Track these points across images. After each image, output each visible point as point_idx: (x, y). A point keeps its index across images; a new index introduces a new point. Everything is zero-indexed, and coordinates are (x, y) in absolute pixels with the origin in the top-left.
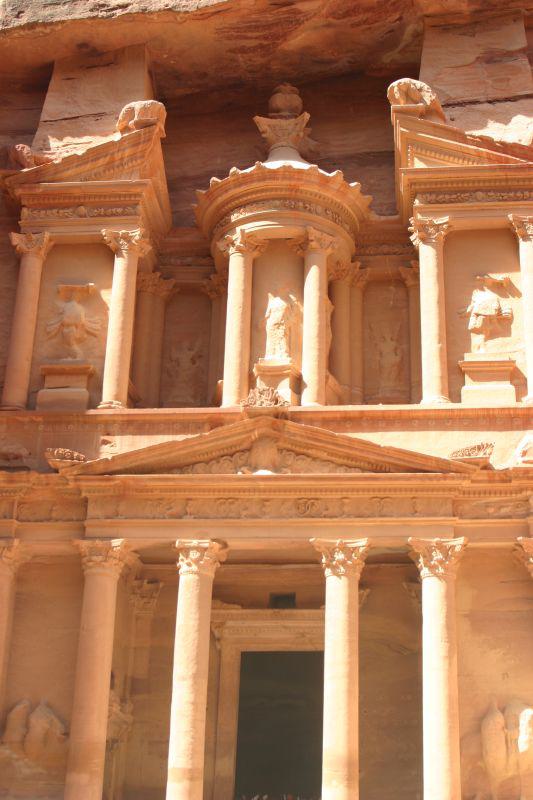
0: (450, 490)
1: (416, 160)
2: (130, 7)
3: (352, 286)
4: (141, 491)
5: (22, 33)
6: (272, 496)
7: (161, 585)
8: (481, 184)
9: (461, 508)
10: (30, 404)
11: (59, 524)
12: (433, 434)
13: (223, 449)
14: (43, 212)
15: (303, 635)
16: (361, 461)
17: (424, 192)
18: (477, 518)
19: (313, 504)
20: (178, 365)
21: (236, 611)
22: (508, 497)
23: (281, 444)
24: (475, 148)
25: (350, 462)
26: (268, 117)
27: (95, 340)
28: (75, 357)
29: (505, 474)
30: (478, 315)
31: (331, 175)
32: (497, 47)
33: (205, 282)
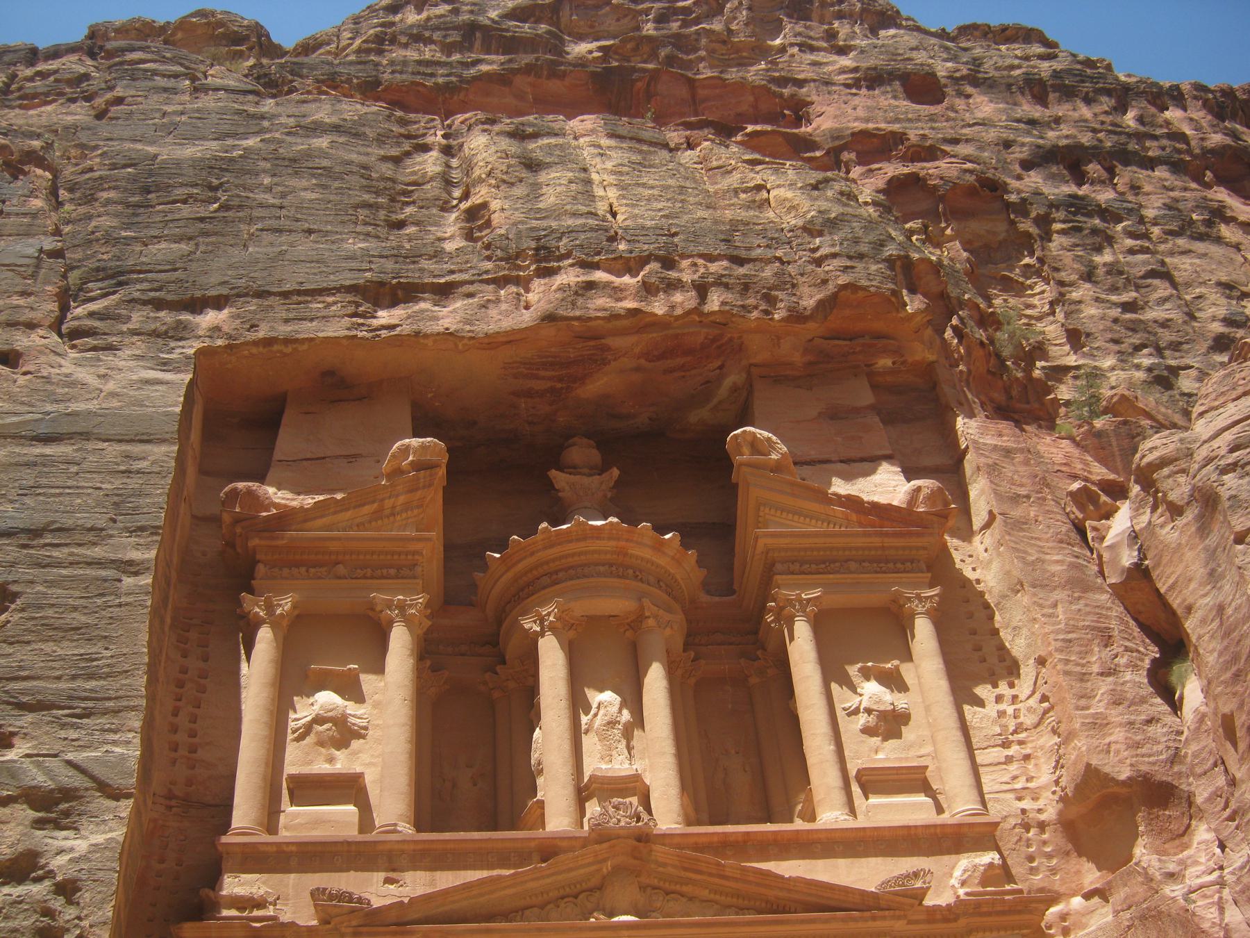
5: (254, 350)
8: (854, 552)
14: (286, 571)
27: (362, 741)
30: (869, 711)
31: (667, 537)
33: (488, 675)
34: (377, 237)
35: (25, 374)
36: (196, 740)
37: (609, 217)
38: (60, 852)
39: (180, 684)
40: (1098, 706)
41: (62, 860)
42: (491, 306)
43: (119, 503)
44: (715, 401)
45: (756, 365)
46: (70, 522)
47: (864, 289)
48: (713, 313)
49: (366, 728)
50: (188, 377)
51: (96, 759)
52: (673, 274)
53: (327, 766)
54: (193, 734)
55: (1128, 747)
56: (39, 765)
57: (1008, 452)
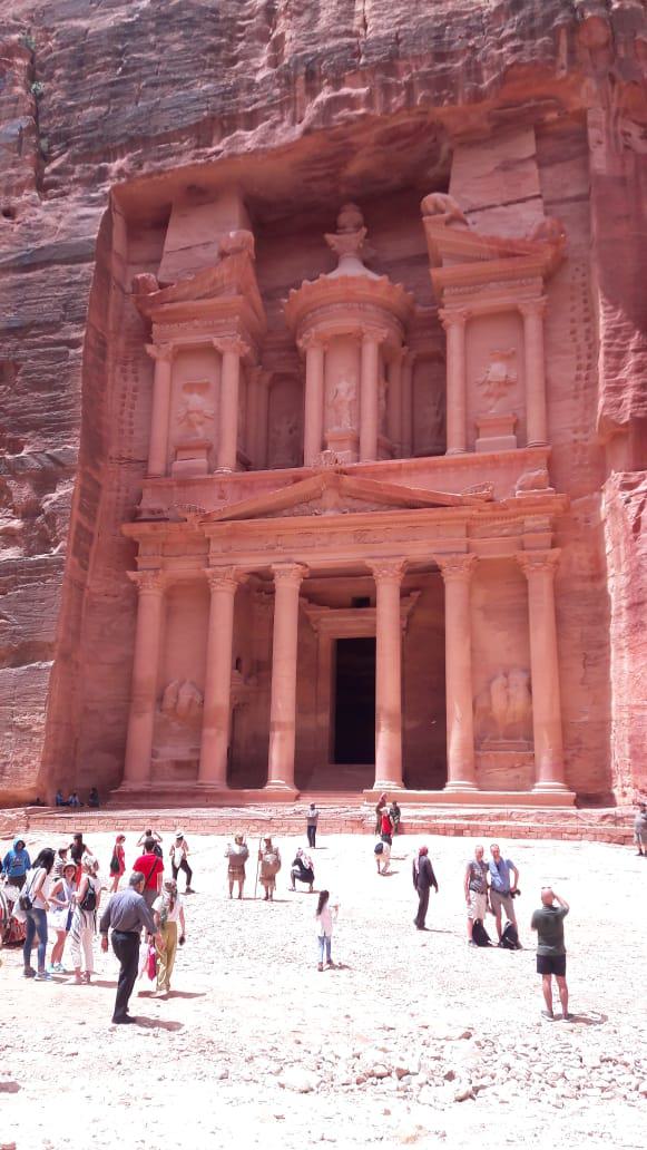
3: (403, 365)
10: (167, 474)
11: (193, 557)
21: (326, 610)
22: (508, 521)
30: (490, 382)
33: (296, 371)
34: (216, 77)
35: (18, 223)
37: (362, 31)
38: (47, 500)
40: (623, 375)
41: (47, 503)
43: (67, 305)
44: (441, 162)
45: (457, 135)
46: (42, 319)
50: (104, 210)
51: (60, 452)
52: (392, 80)
55: (634, 401)
56: (35, 458)
57: (623, 181)
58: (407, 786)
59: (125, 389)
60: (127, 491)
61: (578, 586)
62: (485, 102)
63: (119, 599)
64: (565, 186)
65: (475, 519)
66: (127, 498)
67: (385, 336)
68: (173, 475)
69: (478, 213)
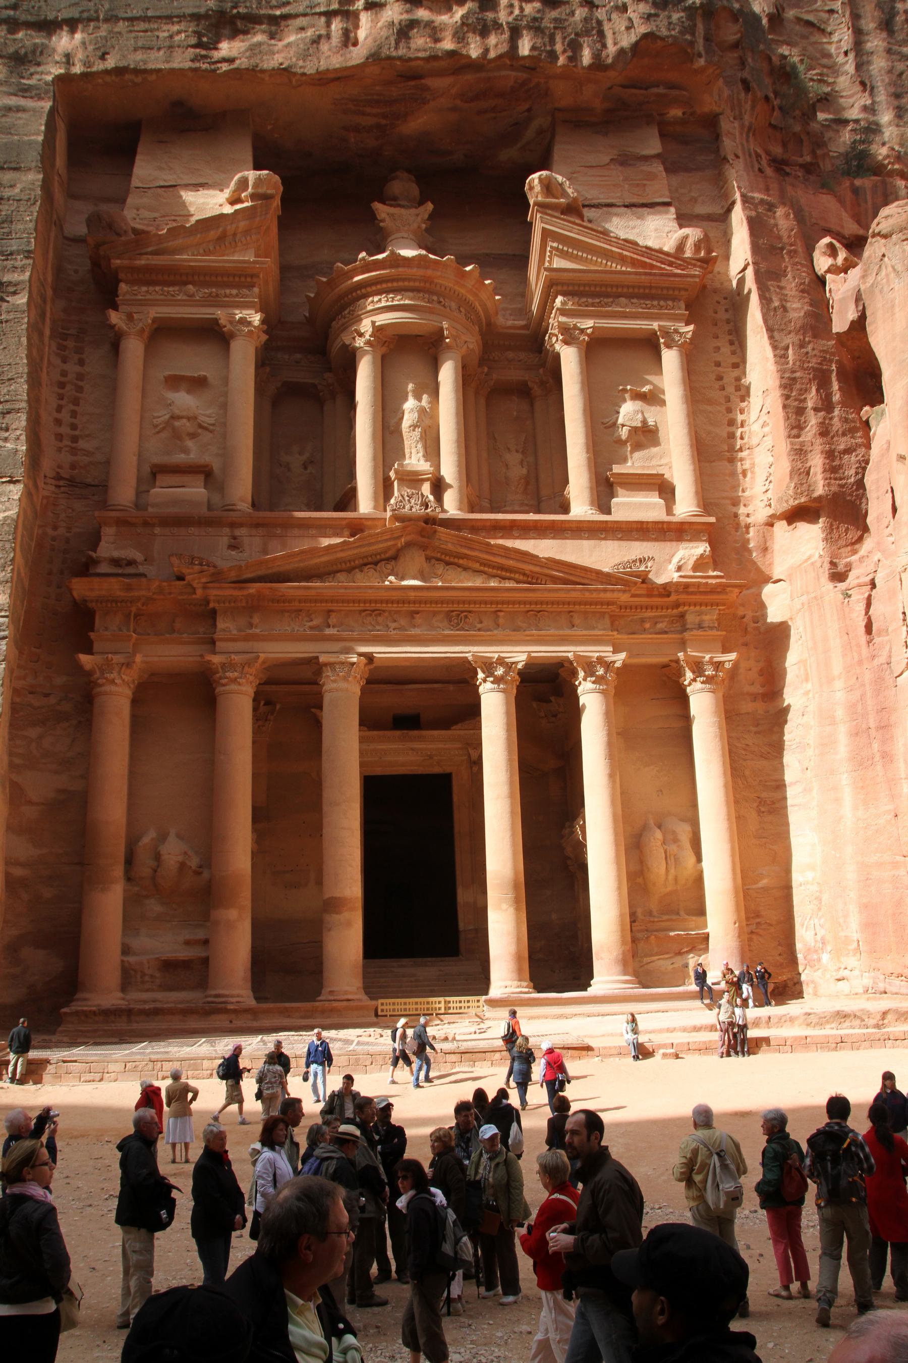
0: (608, 604)
1: (556, 259)
2: (238, 62)
4: (278, 602)
5: (108, 79)
6: (423, 608)
7: (278, 706)
9: (617, 623)
12: (586, 544)
13: (366, 557)
14: (144, 289)
15: (431, 757)
16: (516, 572)
17: (564, 294)
18: (634, 633)
19: (466, 617)
20: (289, 470)
23: (429, 552)
24: (620, 251)
25: (504, 573)
26: (384, 204)
27: (211, 435)
28: (188, 455)
29: (664, 588)
30: (623, 426)
31: (468, 269)
32: (631, 149)
36: (77, 433)
39: (62, 385)
42: (323, 41)
45: (559, 110)
47: (662, 39)
48: (524, 58)
49: (213, 425)
50: (47, 105)
52: (490, 15)
53: (183, 456)
54: (74, 427)
55: (825, 471)
58: (539, 987)
59: (64, 374)
60: (69, 529)
61: (747, 706)
62: (611, 74)
63: (53, 700)
64: (694, 200)
65: (621, 608)
66: (67, 541)
67: (471, 346)
68: (150, 509)
69: (593, 209)
